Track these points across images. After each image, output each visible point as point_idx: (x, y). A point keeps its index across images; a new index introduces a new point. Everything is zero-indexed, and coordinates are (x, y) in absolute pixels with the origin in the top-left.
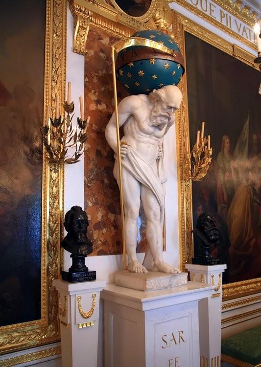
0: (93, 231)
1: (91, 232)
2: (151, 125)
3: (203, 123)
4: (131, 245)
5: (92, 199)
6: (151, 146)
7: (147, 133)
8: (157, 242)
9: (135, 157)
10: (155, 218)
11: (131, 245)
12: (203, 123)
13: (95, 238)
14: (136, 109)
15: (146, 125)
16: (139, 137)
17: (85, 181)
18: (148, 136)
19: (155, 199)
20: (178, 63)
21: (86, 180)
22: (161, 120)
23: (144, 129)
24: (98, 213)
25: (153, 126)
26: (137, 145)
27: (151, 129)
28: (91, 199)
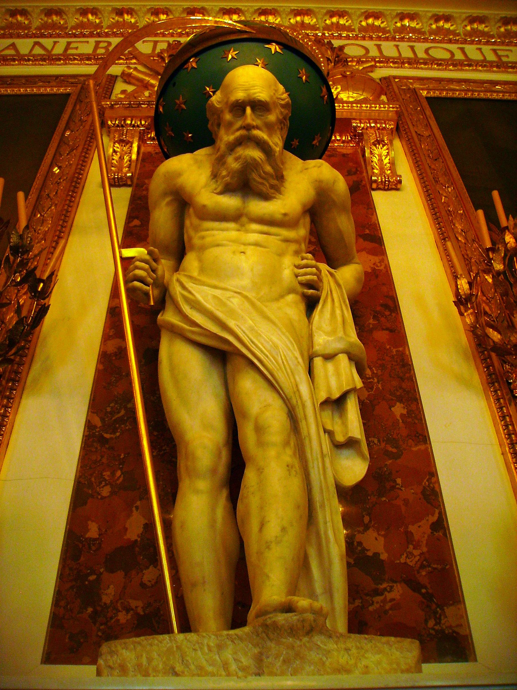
0: (99, 575)
1: (92, 578)
2: (218, 190)
3: (495, 194)
4: (194, 585)
5: (113, 473)
6: (250, 250)
7: (222, 217)
8: (262, 525)
9: (189, 285)
10: (261, 444)
11: (194, 585)
12: (495, 194)
13: (106, 599)
14: (179, 174)
15: (208, 197)
16: (203, 238)
17: (89, 425)
18: (231, 225)
19: (258, 377)
20: (269, 42)
21: (99, 424)
22: (237, 159)
23: (204, 206)
24: (129, 516)
25: (228, 190)
26: (200, 260)
27: (230, 202)
28: (107, 474)
